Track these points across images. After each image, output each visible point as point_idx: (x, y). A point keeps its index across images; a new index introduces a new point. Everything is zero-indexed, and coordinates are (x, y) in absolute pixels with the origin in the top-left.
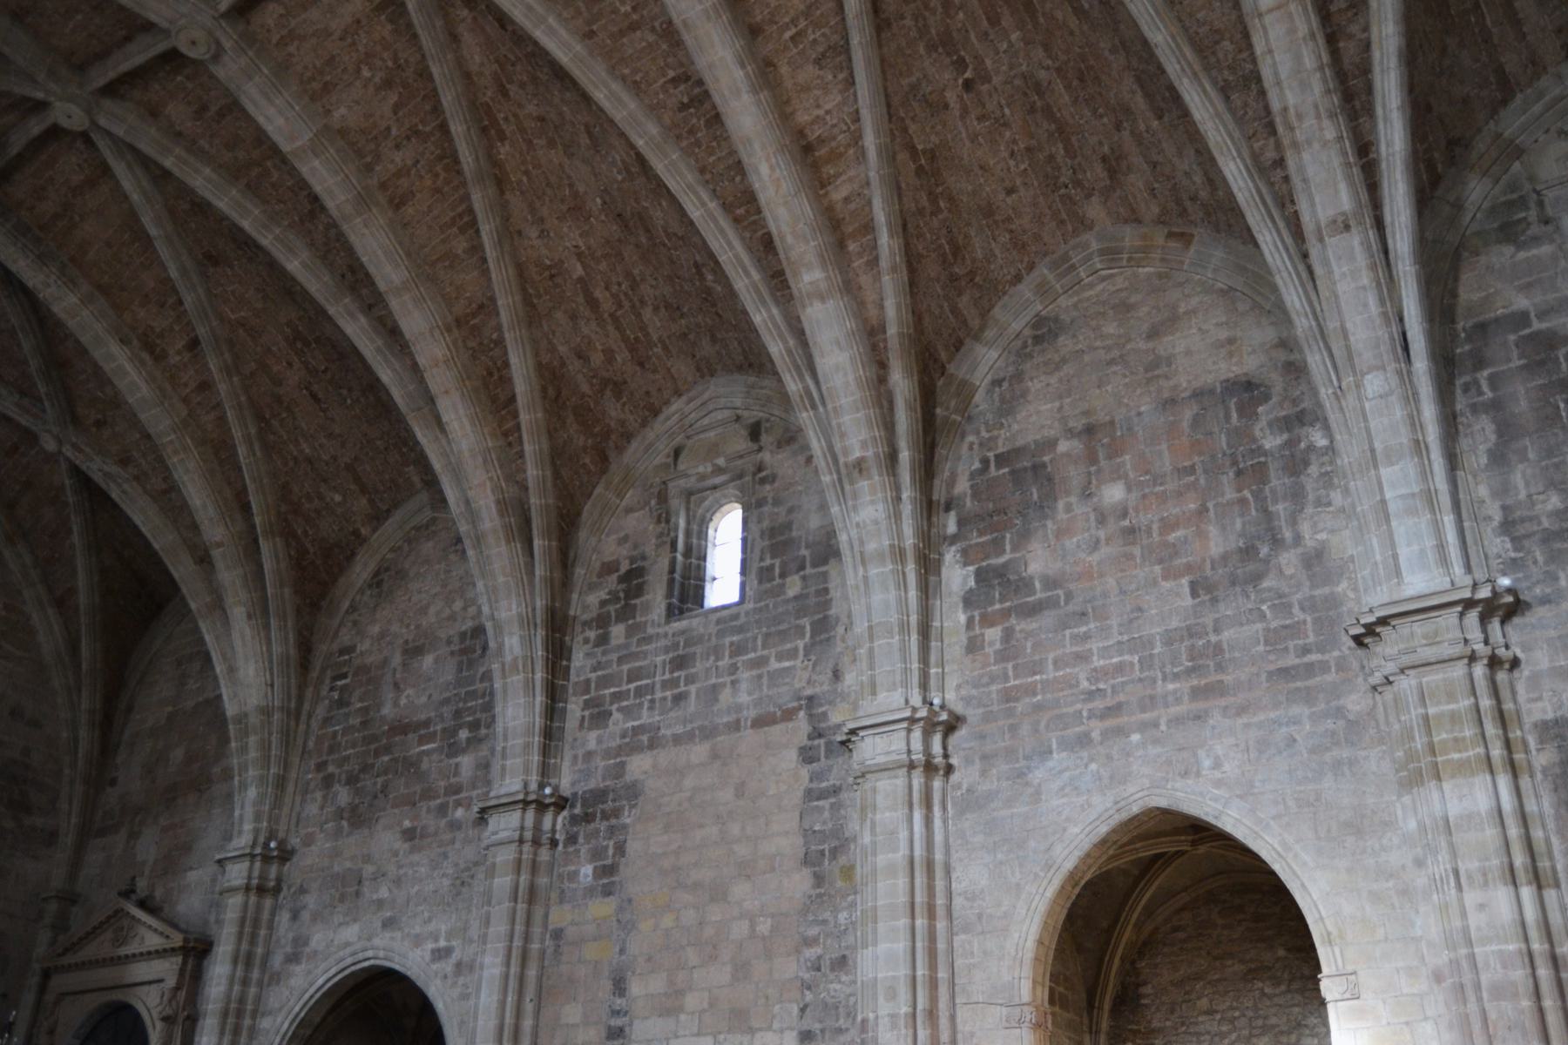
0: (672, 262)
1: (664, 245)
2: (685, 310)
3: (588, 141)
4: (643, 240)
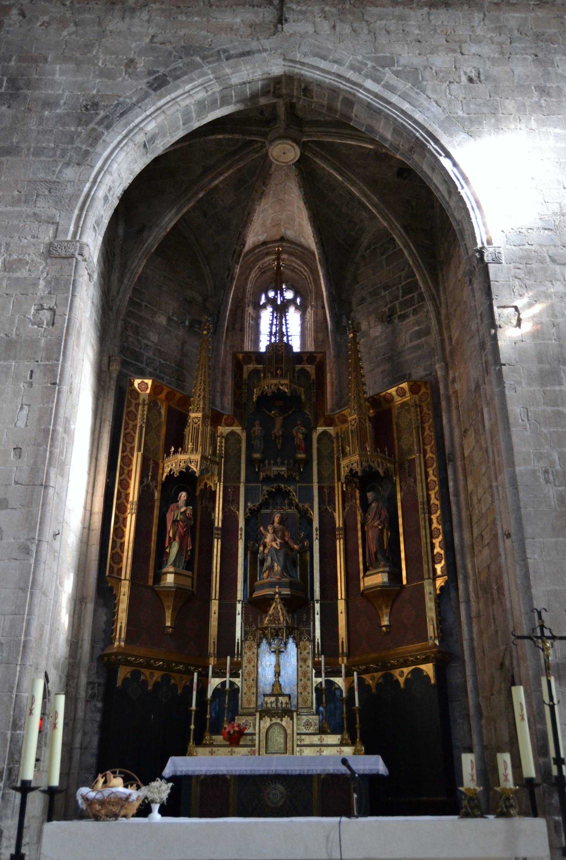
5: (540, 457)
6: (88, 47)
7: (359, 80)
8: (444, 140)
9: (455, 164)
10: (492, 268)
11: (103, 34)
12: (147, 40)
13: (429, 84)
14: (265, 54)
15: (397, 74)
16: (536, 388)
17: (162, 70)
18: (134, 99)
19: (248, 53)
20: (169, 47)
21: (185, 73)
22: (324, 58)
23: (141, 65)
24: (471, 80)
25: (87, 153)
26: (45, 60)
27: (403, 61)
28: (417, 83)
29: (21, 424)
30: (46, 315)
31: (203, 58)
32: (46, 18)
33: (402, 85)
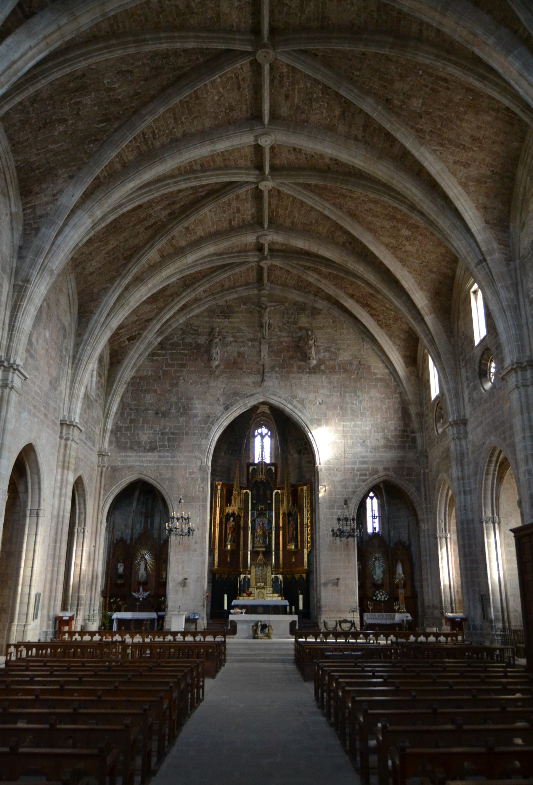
0: (62, 102)
1: (71, 99)
2: (36, 105)
3: (123, 69)
4: (71, 85)
5: (326, 530)
6: (205, 393)
7: (286, 404)
8: (310, 427)
9: (313, 436)
10: (320, 473)
11: (209, 388)
12: (222, 390)
13: (307, 405)
14: (258, 395)
15: (298, 401)
16: (327, 510)
17: (227, 403)
18: (220, 414)
19: (252, 395)
20: (229, 392)
21: (234, 404)
22: (276, 396)
23: (221, 401)
24: (320, 403)
25: (208, 435)
26: (193, 398)
27: (300, 397)
28: (304, 406)
29: (198, 521)
30: (201, 489)
31: (240, 397)
32: (191, 381)
33: (299, 406)
